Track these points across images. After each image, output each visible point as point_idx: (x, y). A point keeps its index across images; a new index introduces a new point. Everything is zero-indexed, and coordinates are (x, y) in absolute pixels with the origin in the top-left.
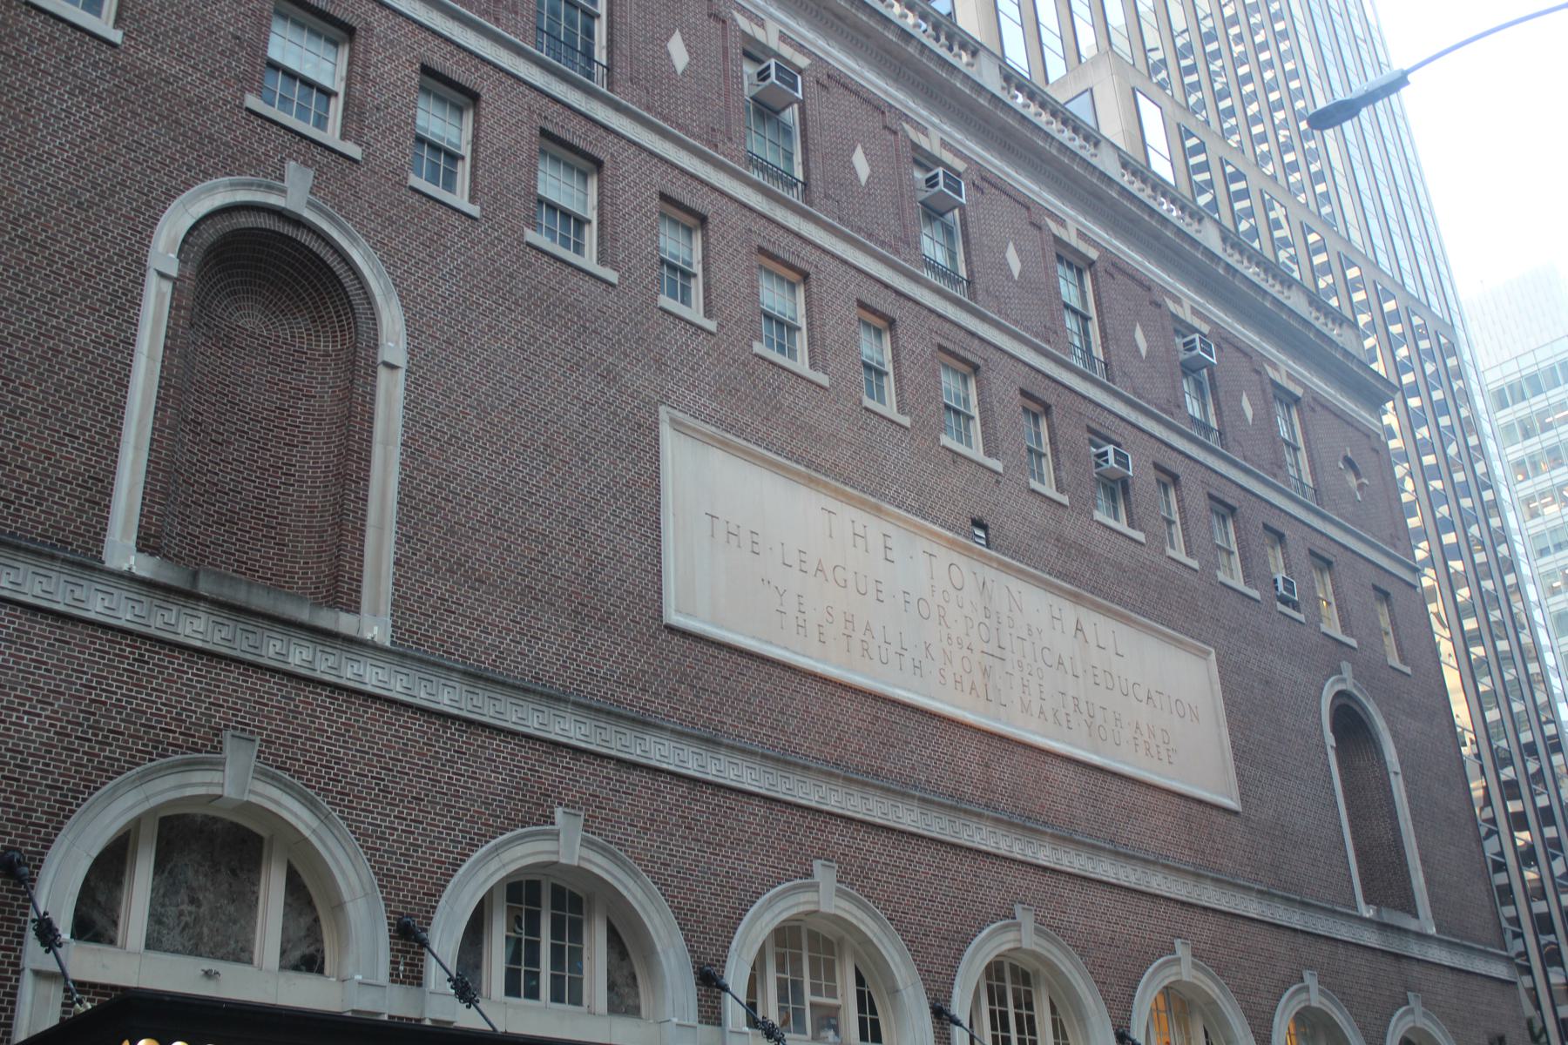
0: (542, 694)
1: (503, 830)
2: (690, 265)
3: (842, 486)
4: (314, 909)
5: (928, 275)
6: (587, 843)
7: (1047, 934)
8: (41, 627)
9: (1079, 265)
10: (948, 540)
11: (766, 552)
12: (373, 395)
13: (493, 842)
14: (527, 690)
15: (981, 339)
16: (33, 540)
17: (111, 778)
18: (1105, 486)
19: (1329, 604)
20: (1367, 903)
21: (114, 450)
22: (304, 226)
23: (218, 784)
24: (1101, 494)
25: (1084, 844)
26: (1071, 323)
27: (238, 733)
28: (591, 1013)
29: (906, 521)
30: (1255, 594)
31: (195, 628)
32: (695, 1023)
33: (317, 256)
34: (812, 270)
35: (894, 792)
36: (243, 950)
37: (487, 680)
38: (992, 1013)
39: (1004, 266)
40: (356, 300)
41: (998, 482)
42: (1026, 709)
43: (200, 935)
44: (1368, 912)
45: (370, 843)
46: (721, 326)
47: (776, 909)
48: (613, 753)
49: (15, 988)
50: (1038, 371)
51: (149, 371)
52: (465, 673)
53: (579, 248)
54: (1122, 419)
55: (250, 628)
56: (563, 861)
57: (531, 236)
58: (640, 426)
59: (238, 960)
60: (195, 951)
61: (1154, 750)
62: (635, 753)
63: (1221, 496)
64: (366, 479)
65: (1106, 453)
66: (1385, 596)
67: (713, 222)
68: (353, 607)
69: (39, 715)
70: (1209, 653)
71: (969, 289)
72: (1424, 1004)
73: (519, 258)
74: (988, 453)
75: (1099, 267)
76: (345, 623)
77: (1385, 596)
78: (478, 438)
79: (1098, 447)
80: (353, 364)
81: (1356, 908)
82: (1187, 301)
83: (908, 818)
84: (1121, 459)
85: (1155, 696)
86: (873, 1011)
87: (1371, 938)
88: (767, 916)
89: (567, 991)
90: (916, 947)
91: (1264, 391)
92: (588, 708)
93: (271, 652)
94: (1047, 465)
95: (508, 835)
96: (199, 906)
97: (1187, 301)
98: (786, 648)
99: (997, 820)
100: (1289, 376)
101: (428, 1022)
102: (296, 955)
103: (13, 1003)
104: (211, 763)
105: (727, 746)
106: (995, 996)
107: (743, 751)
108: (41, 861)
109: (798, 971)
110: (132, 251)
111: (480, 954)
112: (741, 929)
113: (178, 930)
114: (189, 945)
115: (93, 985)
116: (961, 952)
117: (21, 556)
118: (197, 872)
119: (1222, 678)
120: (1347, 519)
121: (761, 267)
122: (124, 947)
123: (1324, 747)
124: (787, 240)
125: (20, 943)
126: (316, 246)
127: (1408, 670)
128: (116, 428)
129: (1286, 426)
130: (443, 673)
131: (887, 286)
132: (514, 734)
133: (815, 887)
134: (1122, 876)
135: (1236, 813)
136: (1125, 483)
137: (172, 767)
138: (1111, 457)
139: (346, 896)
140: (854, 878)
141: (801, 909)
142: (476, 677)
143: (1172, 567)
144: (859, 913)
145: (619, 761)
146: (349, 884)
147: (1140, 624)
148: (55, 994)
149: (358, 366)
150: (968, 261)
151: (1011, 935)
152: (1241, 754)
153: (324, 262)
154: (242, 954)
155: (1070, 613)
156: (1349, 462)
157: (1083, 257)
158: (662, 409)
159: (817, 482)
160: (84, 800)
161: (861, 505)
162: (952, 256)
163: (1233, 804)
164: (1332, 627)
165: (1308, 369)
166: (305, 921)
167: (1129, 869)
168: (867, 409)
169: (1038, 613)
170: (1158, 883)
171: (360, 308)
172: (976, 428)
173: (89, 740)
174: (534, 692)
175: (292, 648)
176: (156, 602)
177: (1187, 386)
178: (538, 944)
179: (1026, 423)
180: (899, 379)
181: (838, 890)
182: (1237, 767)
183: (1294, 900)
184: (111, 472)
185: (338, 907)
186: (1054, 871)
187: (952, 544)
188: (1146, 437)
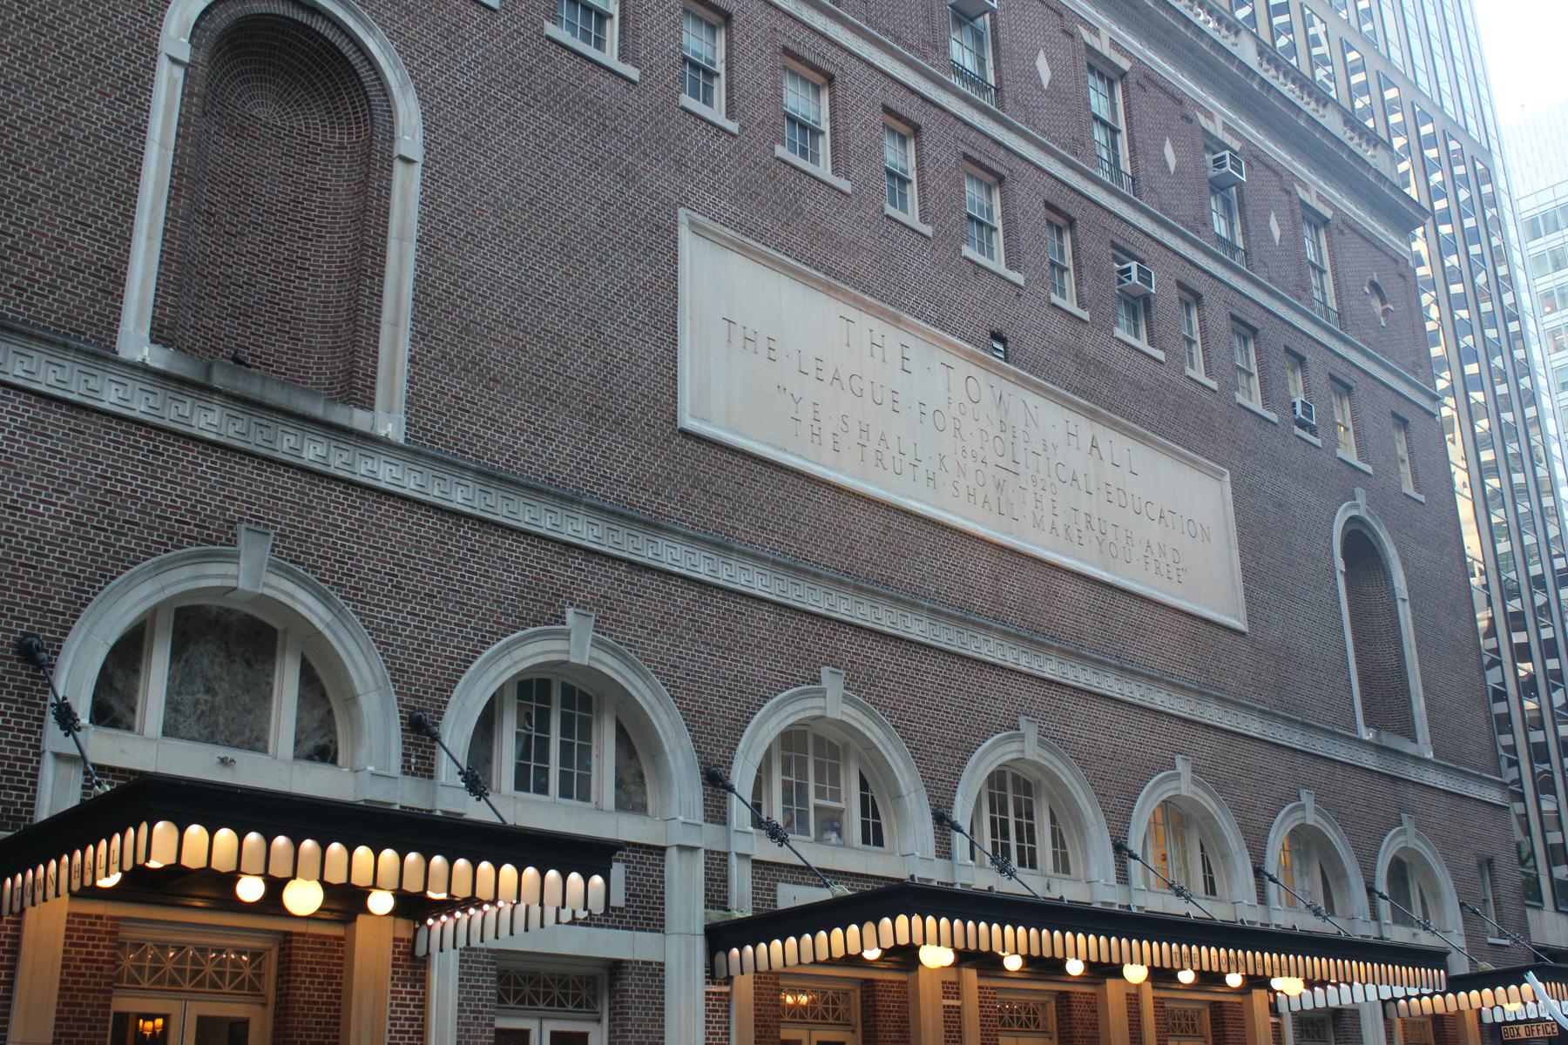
0: (555, 495)
1: (515, 629)
2: (713, 64)
3: (862, 295)
4: (328, 701)
5: (956, 82)
6: (597, 643)
8: (56, 416)
9: (1110, 75)
10: (966, 353)
11: (782, 359)
12: (389, 189)
13: (505, 640)
14: (540, 491)
15: (1008, 149)
16: (46, 329)
17: (127, 568)
18: (1126, 303)
19: (1346, 429)
20: (1367, 727)
21: (127, 240)
22: (319, 13)
23: (232, 577)
24: (1122, 311)
25: (1091, 659)
26: (1099, 135)
27: (252, 526)
28: (599, 809)
29: (923, 332)
30: (1273, 417)
31: (209, 421)
32: (701, 822)
33: (332, 45)
34: (837, 73)
35: (904, 601)
36: (258, 739)
37: (501, 479)
38: (993, 821)
39: (1034, 75)
40: (372, 92)
41: (1019, 295)
42: (1037, 524)
43: (216, 724)
44: (1367, 735)
45: (383, 638)
46: (742, 127)
47: (783, 714)
48: (625, 555)
49: (37, 769)
50: (1064, 183)
51: (161, 159)
52: (479, 473)
53: (599, 44)
54: (1147, 235)
55: (265, 422)
56: (573, 660)
57: (551, 29)
58: (658, 228)
59: (252, 749)
60: (211, 739)
61: (1163, 570)
62: (646, 556)
63: (1243, 317)
64: (381, 275)
65: (1129, 270)
66: (1403, 423)
67: (738, 20)
68: (368, 404)
69: (55, 504)
70: (1223, 475)
71: (998, 96)
72: (1418, 826)
73: (538, 52)
74: (1011, 265)
75: (1131, 78)
76: (359, 419)
77: (1403, 423)
78: (494, 236)
79: (1121, 263)
80: (369, 156)
81: (1356, 731)
82: (1219, 117)
83: (916, 628)
84: (1145, 276)
86: (876, 815)
87: (1369, 761)
88: (775, 720)
89: (576, 787)
90: (920, 756)
91: (1292, 211)
92: (601, 509)
93: (285, 447)
94: (1069, 280)
95: (519, 633)
96: (215, 695)
97: (1219, 117)
98: (800, 456)
99: (1005, 633)
100: (1319, 197)
101: (438, 813)
102: (309, 745)
103: (35, 784)
104: (226, 556)
105: (740, 552)
106: (998, 805)
107: (754, 557)
108: (60, 647)
109: (803, 774)
110: (143, 35)
111: (490, 750)
112: (748, 731)
113: (194, 718)
114: (206, 733)
115: (112, 769)
116: (964, 761)
117: (34, 345)
118: (212, 663)
119: (1235, 500)
120: (1369, 345)
121: (785, 68)
122: (141, 733)
123: (1334, 572)
124: (812, 40)
125: (40, 727)
126: (330, 33)
127: (1422, 498)
128: (129, 216)
129: (1314, 248)
130: (457, 471)
131: (913, 92)
132: (527, 534)
133: (822, 693)
134: (1126, 692)
135: (1243, 634)
136: (1147, 300)
137: (188, 558)
138: (1134, 273)
139: (359, 689)
140: (861, 685)
141: (808, 714)
142: (489, 476)
144: (865, 720)
145: (631, 563)
146: (362, 679)
148: (76, 777)
149: (374, 160)
150: (997, 69)
151: (1015, 746)
152: (1251, 577)
153: (340, 52)
154: (257, 743)
155: (1086, 429)
156: (1375, 287)
157: (1115, 67)
158: (681, 211)
160: (101, 589)
161: (880, 314)
162: (981, 62)
163: (1241, 625)
164: (1349, 453)
165: (1339, 190)
166: (318, 713)
168: (889, 217)
169: (1052, 425)
171: (376, 100)
172: (999, 240)
173: (105, 530)
174: (548, 493)
175: (306, 443)
176: (170, 394)
177: (1214, 204)
178: (547, 740)
179: (1049, 236)
180: (922, 187)
181: (845, 696)
182: (1246, 589)
183: (1296, 721)
184: (124, 261)
185: (351, 699)
186: (1059, 684)
187: (970, 356)
188: (1170, 255)
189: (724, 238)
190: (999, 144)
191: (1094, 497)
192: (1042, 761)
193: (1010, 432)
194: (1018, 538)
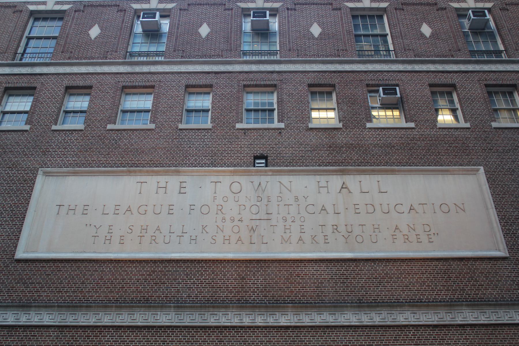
5: (142, 59)
10: (231, 171)
61: (413, 238)
70: (478, 170)
83: (164, 318)
85: (420, 209)
98: (95, 252)
105: (35, 306)
135: (504, 259)
143: (445, 132)
147: (399, 171)
157: (378, 9)
159: (135, 172)
163: (502, 252)
167: (373, 314)
170: (405, 317)
189: (64, 172)
190: (272, 72)
193: (265, 201)
194: (266, 253)
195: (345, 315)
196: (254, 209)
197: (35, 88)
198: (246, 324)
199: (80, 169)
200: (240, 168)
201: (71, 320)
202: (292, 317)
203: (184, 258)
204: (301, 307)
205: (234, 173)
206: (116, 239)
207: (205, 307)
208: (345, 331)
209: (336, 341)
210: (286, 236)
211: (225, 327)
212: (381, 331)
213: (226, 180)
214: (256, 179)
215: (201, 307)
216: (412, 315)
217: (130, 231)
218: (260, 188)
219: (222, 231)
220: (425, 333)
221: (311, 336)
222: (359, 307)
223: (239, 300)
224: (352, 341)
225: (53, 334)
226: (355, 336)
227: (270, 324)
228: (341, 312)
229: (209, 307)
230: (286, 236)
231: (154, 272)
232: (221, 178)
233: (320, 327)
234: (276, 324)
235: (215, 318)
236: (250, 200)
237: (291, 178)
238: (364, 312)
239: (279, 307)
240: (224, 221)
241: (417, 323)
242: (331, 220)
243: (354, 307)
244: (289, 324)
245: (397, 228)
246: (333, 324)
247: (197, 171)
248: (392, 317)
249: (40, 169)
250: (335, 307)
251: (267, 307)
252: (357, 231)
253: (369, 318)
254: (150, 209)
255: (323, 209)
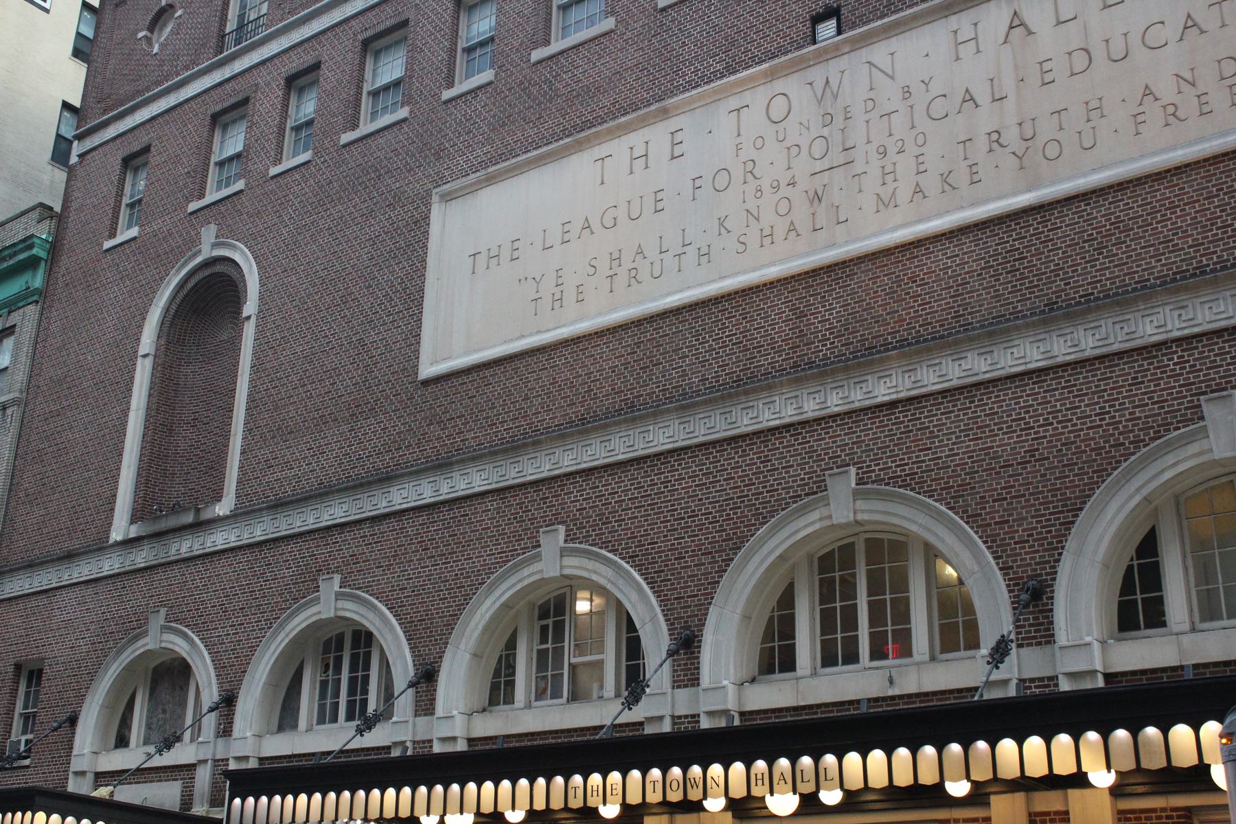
7: (878, 492)
37: (282, 505)
52: (268, 508)
56: (324, 616)
83: (663, 436)
98: (539, 332)
105: (458, 462)
133: (537, 558)
134: (1047, 354)
144: (590, 564)
145: (375, 519)
159: (588, 139)
189: (471, 185)
191: (1010, 104)
192: (866, 517)
193: (839, 121)
195: (1015, 350)
196: (818, 149)
197: (404, 24)
198: (810, 415)
199: (498, 167)
200: (784, 58)
201: (513, 475)
202: (900, 379)
203: (712, 294)
204: (918, 353)
205: (772, 75)
206: (570, 295)
207: (730, 396)
208: (1016, 387)
209: (997, 413)
210: (886, 193)
211: (772, 430)
212: (1099, 369)
213: (757, 98)
214: (817, 74)
215: (722, 398)
216: (1176, 313)
217: (592, 270)
218: (828, 90)
219: (758, 219)
220: (1209, 351)
221: (942, 414)
222: (1044, 322)
223: (796, 366)
224: (1032, 405)
225: (492, 504)
226: (1039, 393)
227: (857, 405)
228: (1005, 345)
229: (737, 394)
230: (886, 193)
231: (638, 344)
232: (747, 97)
233: (960, 389)
234: (867, 403)
235: (750, 415)
236: (808, 129)
237: (894, 44)
238: (1059, 333)
239: (871, 363)
240: (759, 194)
241: (1186, 332)
242: (985, 119)
243: (1034, 324)
244: (894, 397)
245: (1148, 92)
246: (987, 376)
247: (700, 97)
248: (1126, 330)
249: (434, 191)
250: (991, 334)
251: (846, 369)
252: (1047, 129)
253: (1069, 344)
254: (621, 213)
255: (969, 98)
